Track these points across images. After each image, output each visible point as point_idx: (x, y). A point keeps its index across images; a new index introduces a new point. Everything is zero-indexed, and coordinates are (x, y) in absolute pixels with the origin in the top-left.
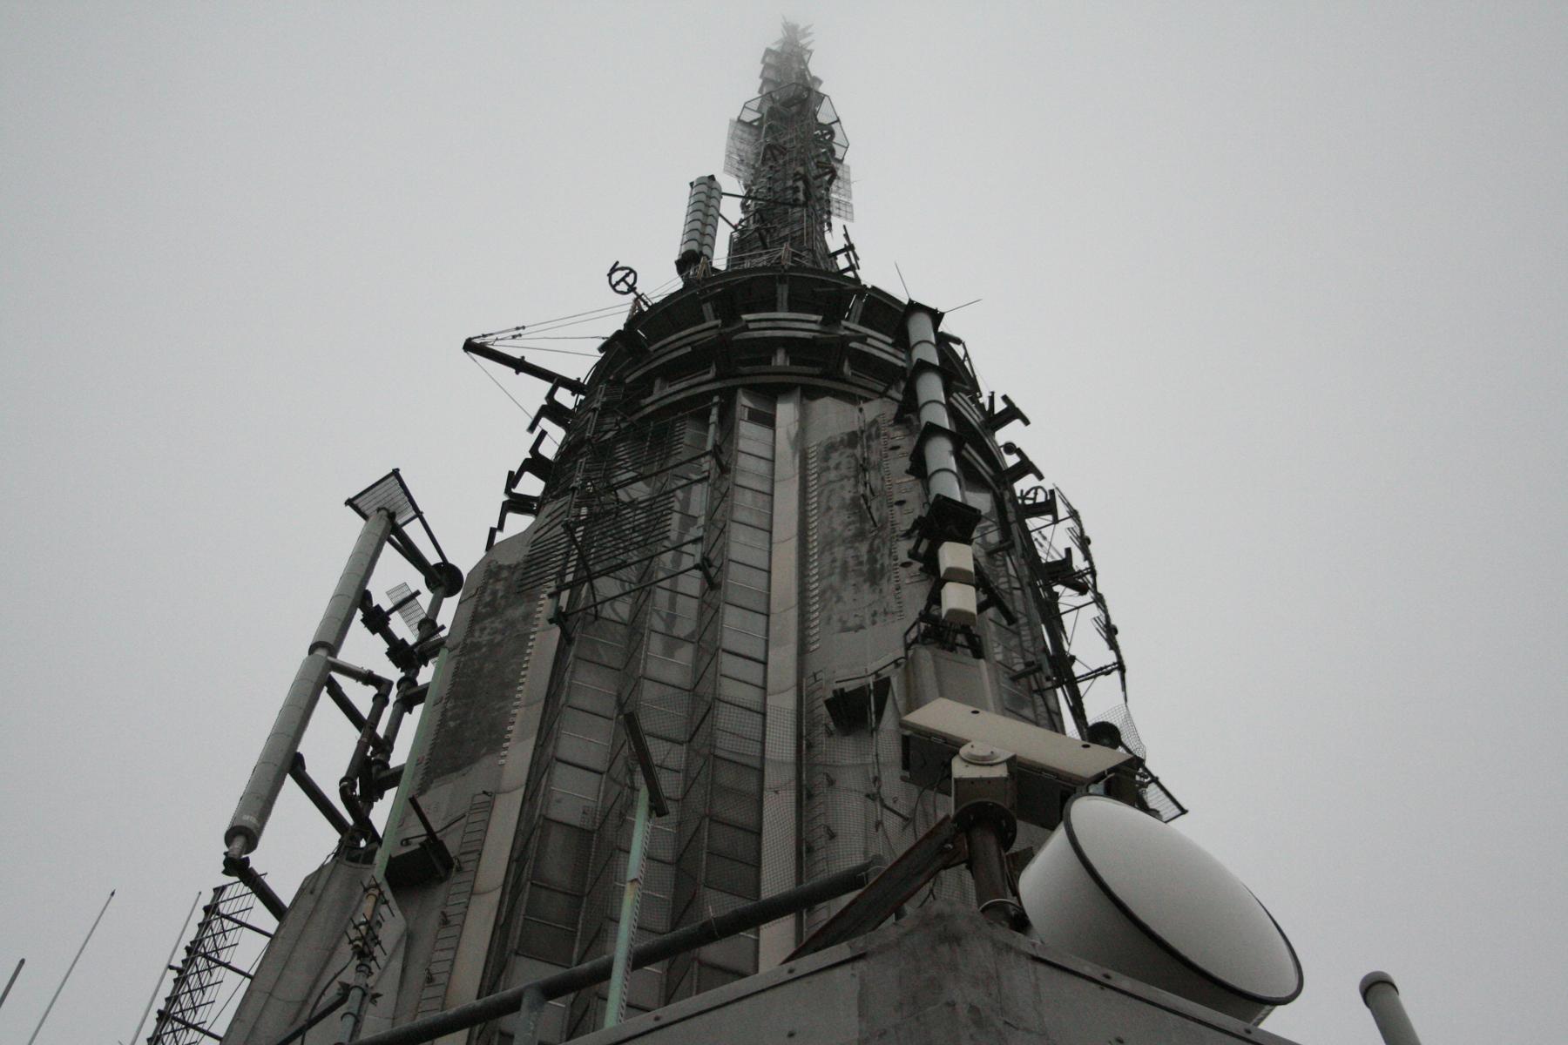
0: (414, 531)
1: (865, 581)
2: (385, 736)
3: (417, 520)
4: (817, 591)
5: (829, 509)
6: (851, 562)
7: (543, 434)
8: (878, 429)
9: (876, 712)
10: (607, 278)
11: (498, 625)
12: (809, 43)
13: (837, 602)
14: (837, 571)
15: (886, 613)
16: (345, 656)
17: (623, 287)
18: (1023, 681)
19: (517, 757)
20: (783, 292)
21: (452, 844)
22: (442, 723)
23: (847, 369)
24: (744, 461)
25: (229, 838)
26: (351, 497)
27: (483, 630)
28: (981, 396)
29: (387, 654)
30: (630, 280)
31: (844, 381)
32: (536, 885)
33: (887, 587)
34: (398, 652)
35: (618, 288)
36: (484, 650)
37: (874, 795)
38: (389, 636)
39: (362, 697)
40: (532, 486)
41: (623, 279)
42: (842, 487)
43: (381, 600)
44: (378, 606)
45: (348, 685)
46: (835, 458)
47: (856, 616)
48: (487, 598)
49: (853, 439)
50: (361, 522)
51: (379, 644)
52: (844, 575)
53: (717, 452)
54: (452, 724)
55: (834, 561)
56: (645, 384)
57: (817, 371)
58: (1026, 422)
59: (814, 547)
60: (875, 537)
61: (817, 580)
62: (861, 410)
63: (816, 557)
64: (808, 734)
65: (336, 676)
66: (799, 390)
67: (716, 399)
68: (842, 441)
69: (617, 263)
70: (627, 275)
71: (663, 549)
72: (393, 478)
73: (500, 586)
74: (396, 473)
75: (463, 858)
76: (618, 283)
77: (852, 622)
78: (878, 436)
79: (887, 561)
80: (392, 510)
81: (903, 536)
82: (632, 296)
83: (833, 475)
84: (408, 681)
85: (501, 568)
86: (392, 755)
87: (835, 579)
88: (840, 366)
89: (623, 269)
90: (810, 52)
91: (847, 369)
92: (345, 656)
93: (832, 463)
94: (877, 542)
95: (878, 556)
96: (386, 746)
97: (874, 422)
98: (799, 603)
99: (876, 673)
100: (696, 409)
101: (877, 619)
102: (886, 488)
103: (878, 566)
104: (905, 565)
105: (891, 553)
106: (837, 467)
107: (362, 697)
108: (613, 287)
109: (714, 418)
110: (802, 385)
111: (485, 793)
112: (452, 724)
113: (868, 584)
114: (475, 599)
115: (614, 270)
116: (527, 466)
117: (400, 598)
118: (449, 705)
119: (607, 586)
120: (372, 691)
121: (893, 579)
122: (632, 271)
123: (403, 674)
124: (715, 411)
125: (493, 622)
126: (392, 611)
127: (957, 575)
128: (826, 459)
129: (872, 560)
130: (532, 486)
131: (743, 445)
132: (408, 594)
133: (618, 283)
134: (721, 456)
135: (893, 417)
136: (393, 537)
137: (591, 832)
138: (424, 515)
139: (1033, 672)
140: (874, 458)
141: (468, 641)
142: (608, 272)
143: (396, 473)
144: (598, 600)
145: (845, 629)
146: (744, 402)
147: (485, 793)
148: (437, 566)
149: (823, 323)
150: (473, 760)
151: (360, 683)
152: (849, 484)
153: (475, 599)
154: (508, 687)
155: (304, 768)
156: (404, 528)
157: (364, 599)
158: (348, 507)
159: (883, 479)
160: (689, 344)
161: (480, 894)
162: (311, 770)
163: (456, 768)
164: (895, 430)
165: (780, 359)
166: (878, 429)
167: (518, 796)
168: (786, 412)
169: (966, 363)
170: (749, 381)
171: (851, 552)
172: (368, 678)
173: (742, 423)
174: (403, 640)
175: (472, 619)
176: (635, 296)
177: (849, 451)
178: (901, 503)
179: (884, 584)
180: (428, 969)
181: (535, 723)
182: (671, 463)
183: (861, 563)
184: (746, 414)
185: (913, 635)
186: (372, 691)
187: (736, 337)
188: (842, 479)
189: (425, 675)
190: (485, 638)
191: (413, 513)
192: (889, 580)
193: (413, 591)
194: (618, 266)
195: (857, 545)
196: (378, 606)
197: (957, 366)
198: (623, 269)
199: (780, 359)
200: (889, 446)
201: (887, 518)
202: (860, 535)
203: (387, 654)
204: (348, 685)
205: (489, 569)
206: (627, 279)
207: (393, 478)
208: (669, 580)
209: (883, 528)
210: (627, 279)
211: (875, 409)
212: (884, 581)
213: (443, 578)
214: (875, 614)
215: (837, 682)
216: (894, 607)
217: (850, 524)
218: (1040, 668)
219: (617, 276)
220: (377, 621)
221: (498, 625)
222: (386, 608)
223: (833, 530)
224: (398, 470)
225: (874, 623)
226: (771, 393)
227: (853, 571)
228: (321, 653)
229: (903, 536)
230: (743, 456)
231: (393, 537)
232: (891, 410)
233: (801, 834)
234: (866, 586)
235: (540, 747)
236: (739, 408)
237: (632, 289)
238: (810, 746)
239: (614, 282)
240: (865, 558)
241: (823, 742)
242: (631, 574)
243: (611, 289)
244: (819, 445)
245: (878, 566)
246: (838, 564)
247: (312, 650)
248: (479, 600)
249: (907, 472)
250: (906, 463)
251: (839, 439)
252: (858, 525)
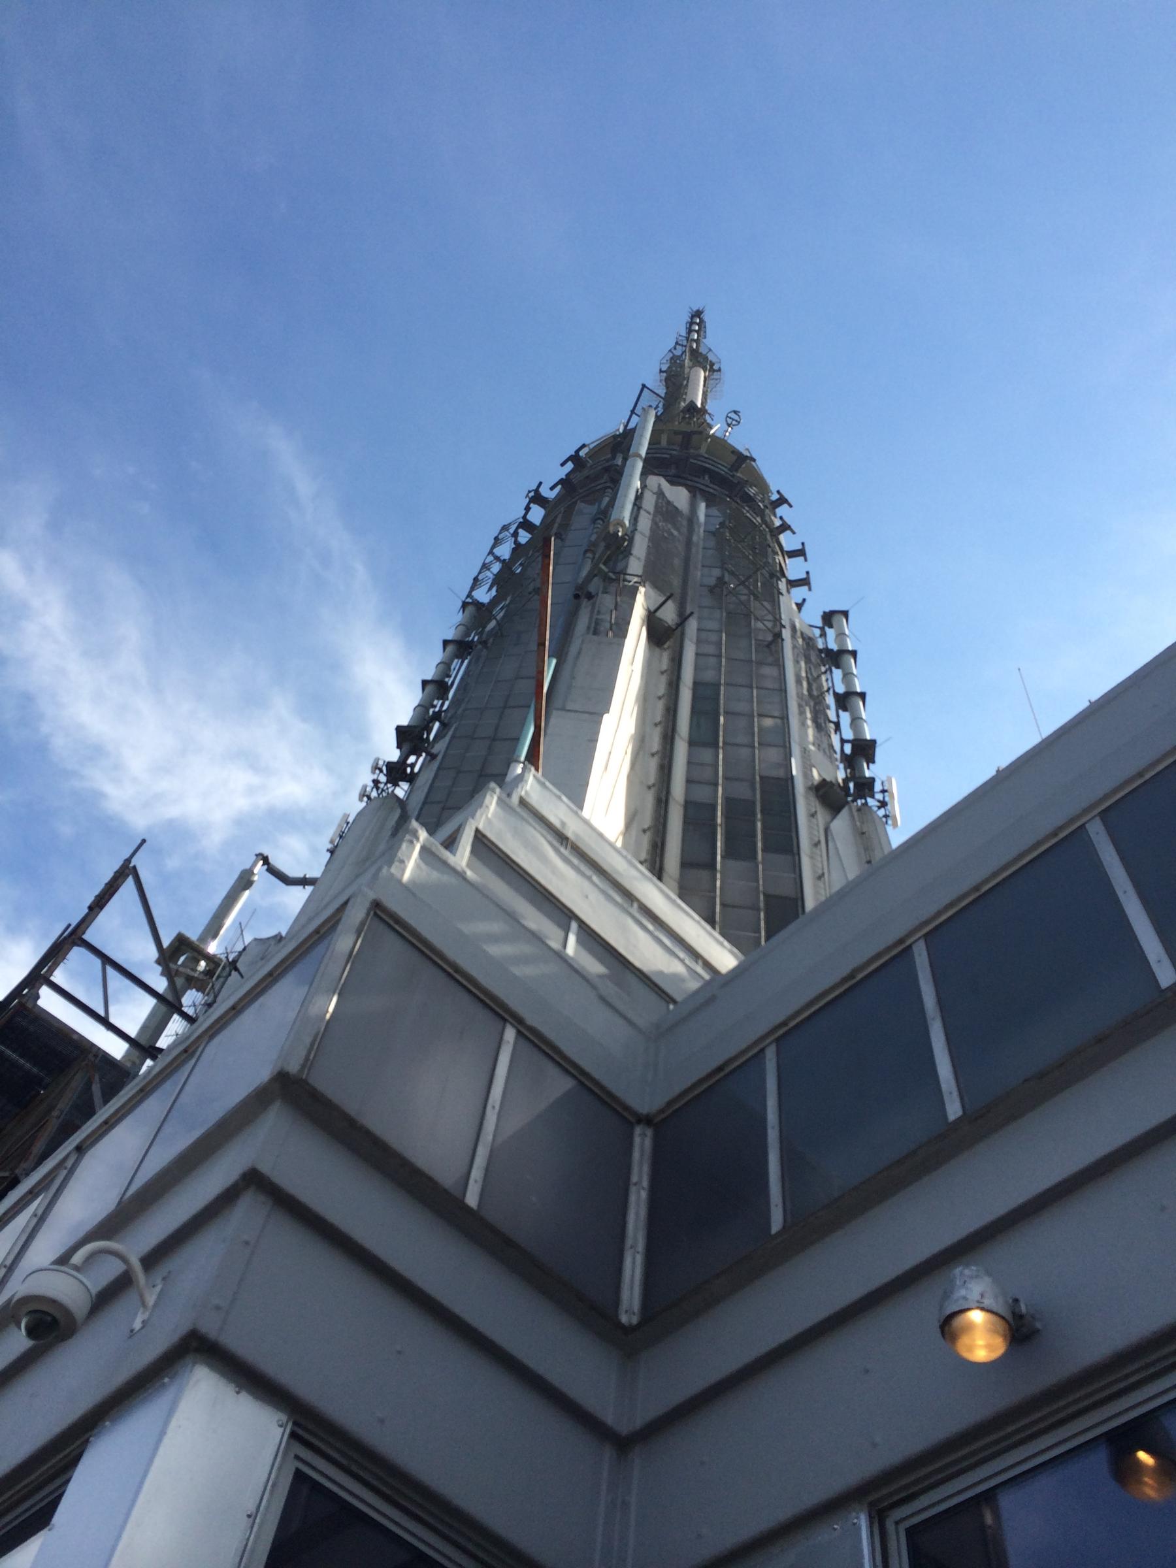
26: (647, 385)
35: (728, 419)
36: (660, 532)
41: (733, 420)
70: (736, 421)
76: (730, 418)
89: (738, 415)
108: (727, 417)
115: (735, 412)
122: (739, 422)
133: (730, 418)
158: (641, 387)
179: (823, 733)
239: (729, 415)
243: (725, 417)
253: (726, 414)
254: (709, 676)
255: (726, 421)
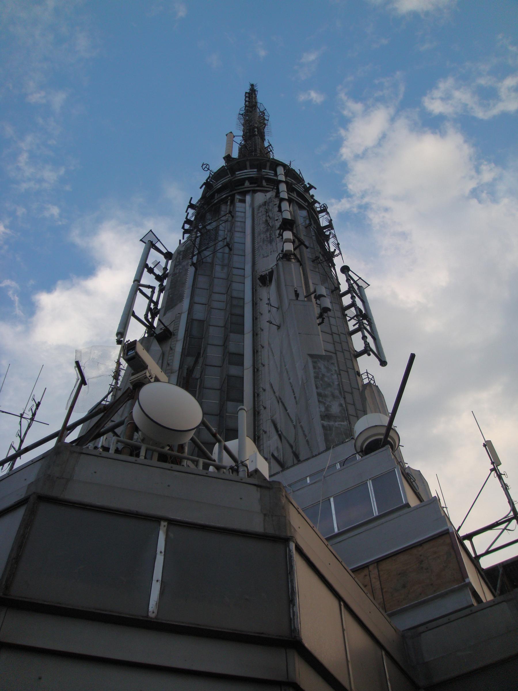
0: (158, 245)
1: (269, 243)
2: (156, 301)
3: (159, 242)
4: (257, 247)
5: (259, 224)
6: (265, 238)
7: (188, 213)
8: (271, 200)
9: (269, 281)
10: (202, 168)
11: (181, 267)
12: (257, 89)
13: (262, 250)
14: (262, 241)
15: (274, 251)
16: (143, 282)
17: (206, 169)
18: (316, 261)
19: (186, 303)
20: (248, 164)
21: (171, 329)
22: (169, 296)
23: (264, 184)
24: (238, 214)
25: (118, 334)
26: (141, 239)
27: (177, 269)
28: (305, 182)
29: (155, 279)
30: (208, 167)
31: (264, 187)
32: (191, 337)
33: (274, 244)
34: (158, 278)
35: (205, 170)
36: (178, 274)
37: (268, 303)
38: (155, 274)
39: (148, 292)
40: (187, 227)
41: (206, 167)
42: (263, 217)
43: (151, 265)
44: (150, 267)
45: (144, 289)
46: (261, 209)
47: (266, 253)
48: (178, 260)
49: (265, 203)
50: (144, 244)
51: (153, 276)
52: (263, 241)
53: (230, 212)
54: (171, 296)
55: (261, 238)
56: (212, 196)
57: (256, 185)
58: (315, 189)
59: (256, 235)
60: (271, 230)
61: (257, 244)
62: (266, 196)
63: (256, 238)
64: (255, 288)
65: (140, 288)
66: (251, 192)
67: (229, 198)
68: (263, 204)
69: (203, 163)
70: (207, 166)
71: (218, 241)
72: (150, 232)
73: (181, 257)
74: (151, 231)
75: (174, 332)
76: (205, 168)
77: (266, 255)
78: (271, 202)
79: (274, 237)
80: (151, 241)
81: (278, 229)
82: (209, 171)
83: (260, 215)
84: (161, 285)
85: (181, 251)
86: (158, 305)
87: (261, 243)
88: (262, 182)
89: (205, 164)
90: (257, 91)
91: (264, 184)
92: (143, 282)
93: (260, 211)
94: (271, 231)
95: (272, 236)
96: (156, 304)
97: (270, 198)
98: (252, 252)
99: (271, 268)
100: (224, 201)
101: (272, 253)
102: (273, 216)
103: (272, 238)
104: (278, 237)
105: (275, 234)
106: (261, 211)
107: (148, 292)
108: (204, 169)
109: (229, 203)
110: (251, 190)
111: (179, 314)
112: (171, 296)
113: (269, 244)
114: (175, 261)
115: (203, 165)
116: (186, 222)
117: (156, 264)
118: (170, 291)
119: (207, 253)
120: (151, 290)
121: (275, 242)
122: (207, 165)
123: (160, 283)
124: (229, 201)
125: (179, 267)
126: (154, 268)
127: (288, 241)
128: (259, 210)
129: (271, 237)
130: (187, 227)
131: (237, 209)
132: (157, 263)
133: (205, 168)
134: (232, 213)
135: (274, 196)
136: (153, 247)
137: (204, 321)
138: (160, 240)
139: (317, 259)
140: (270, 208)
141: (174, 273)
142: (201, 166)
143: (151, 231)
144: (203, 257)
145: (264, 257)
146: (237, 197)
147: (179, 314)
148: (166, 253)
149: (257, 171)
150: (176, 305)
151: (147, 289)
152: (264, 216)
153: (175, 261)
154: (184, 284)
155: (135, 313)
156: (156, 245)
157: (146, 266)
159: (272, 214)
160: (221, 184)
161: (179, 341)
162: (136, 314)
163: (172, 308)
164: (276, 199)
165: (247, 184)
166: (271, 200)
167: (187, 313)
168: (248, 198)
169: (300, 175)
170: (238, 191)
171: (265, 235)
172: (149, 287)
173: (237, 203)
174: (158, 275)
175: (175, 266)
176: (210, 171)
177: (264, 207)
178: (277, 220)
180: (167, 362)
181: (190, 293)
182: (220, 217)
183: (268, 238)
184: (238, 201)
185: (278, 258)
186: (151, 290)
187: (233, 180)
188: (263, 215)
189: (165, 283)
190: (178, 271)
191: (158, 240)
192: (274, 241)
193: (158, 262)
194: (204, 164)
195: (266, 233)
196: (150, 267)
197: (298, 176)
198: (205, 164)
199: (247, 184)
200: (274, 204)
201: (274, 224)
202: (267, 230)
203: (155, 279)
204: (144, 289)
205: (178, 252)
206: (207, 167)
207: (150, 232)
208: (222, 249)
209: (273, 227)
210: (207, 167)
211: (269, 195)
212: (273, 242)
213: (168, 256)
214: (271, 252)
215: (262, 272)
216: (275, 249)
217: (265, 227)
218: (319, 258)
219: (204, 166)
220: (151, 271)
221: (181, 267)
222: (152, 267)
223: (261, 230)
224: (151, 230)
225: (271, 254)
226: (244, 193)
227: (266, 240)
228: (136, 282)
229: (278, 229)
230: (237, 212)
231: (153, 247)
232: (274, 194)
233: (254, 315)
234: (269, 244)
235: (191, 300)
236: (236, 199)
237: (208, 169)
238: (256, 290)
239: (203, 168)
240: (269, 236)
241: (259, 289)
242: (212, 249)
244: (257, 206)
245: (272, 238)
246: (262, 239)
247: (134, 281)
248: (176, 261)
249: (278, 211)
250: (277, 209)
251: (262, 204)
252: (267, 227)
253: (203, 170)
254: (199, 313)
255: (206, 171)
